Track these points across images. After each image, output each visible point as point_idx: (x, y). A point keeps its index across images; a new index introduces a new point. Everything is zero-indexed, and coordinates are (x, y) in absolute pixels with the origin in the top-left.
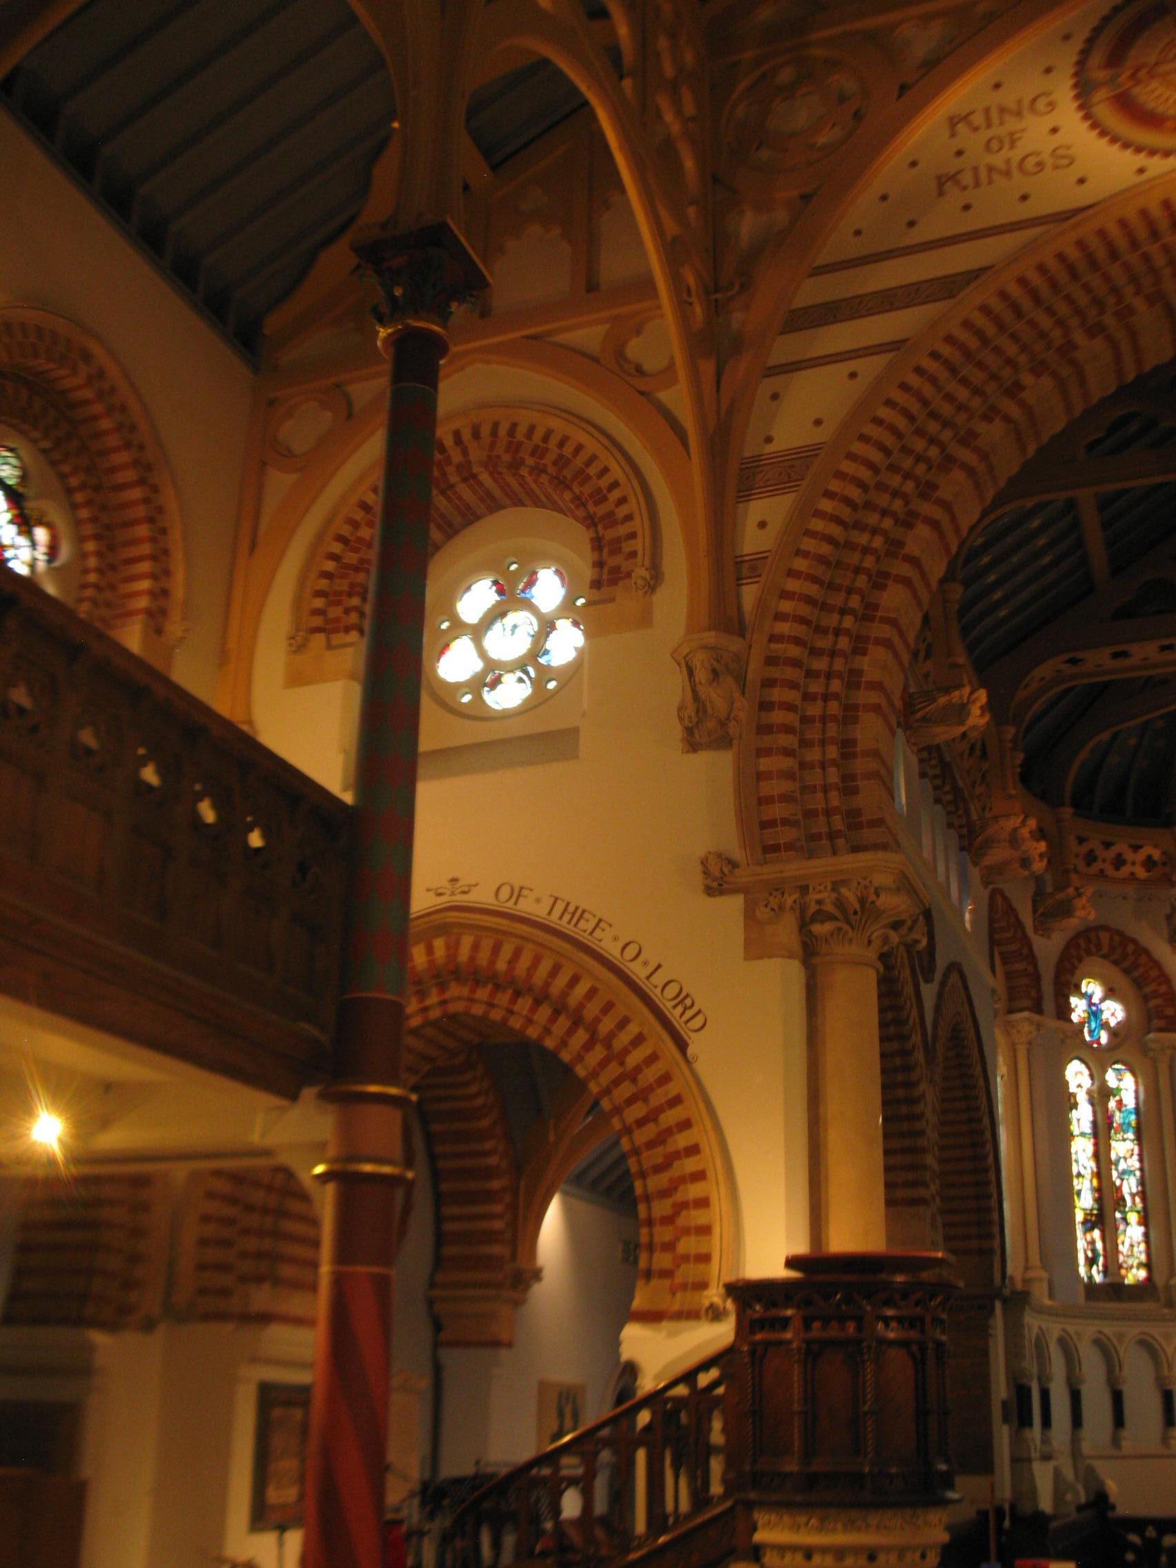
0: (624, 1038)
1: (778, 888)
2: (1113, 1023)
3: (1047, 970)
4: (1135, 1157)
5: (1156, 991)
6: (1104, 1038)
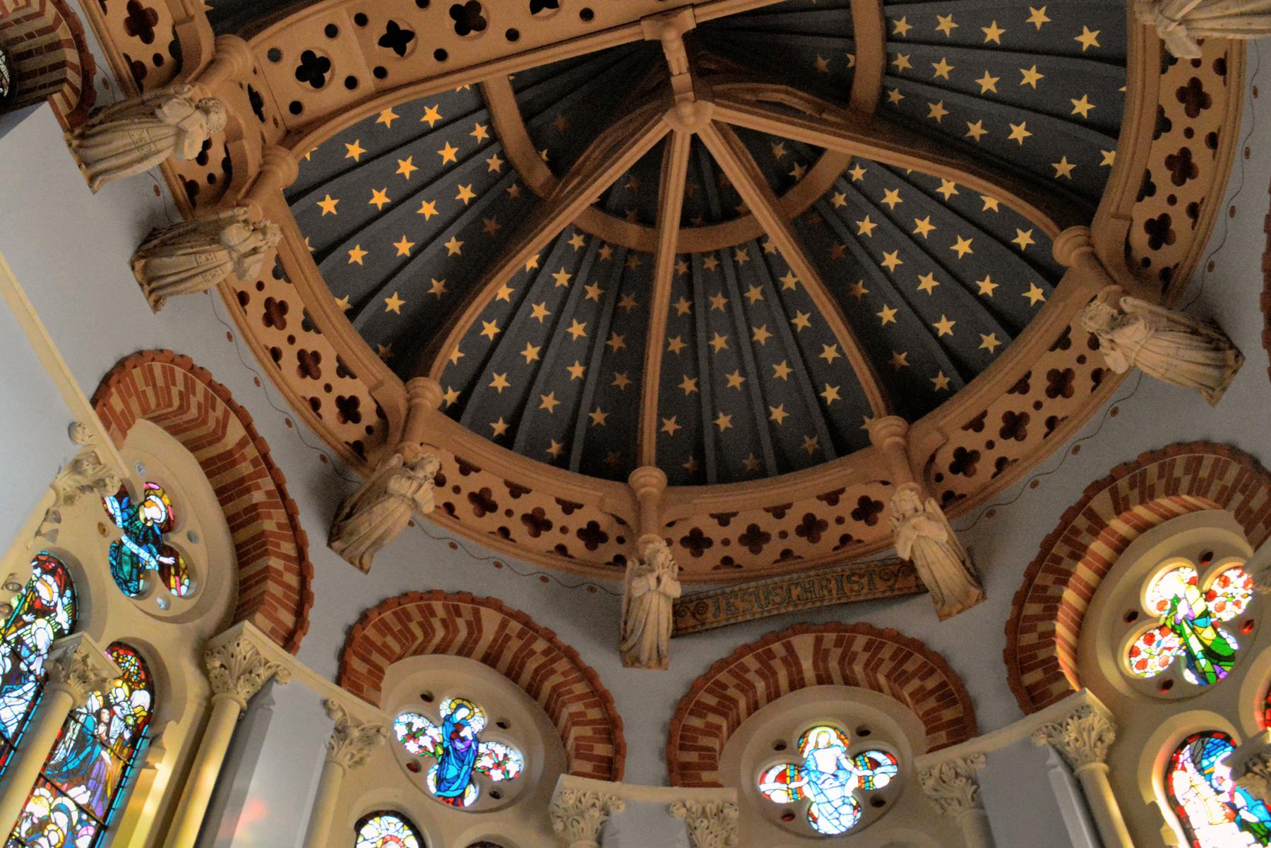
2: (497, 775)
5: (583, 714)
6: (471, 795)
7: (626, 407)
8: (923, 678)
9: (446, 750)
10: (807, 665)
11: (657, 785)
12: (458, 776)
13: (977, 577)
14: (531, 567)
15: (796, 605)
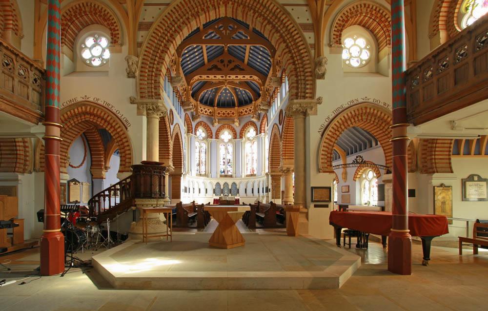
0: (117, 127)
1: (142, 104)
3: (194, 127)
6: (202, 138)
7: (215, 96)
13: (240, 124)
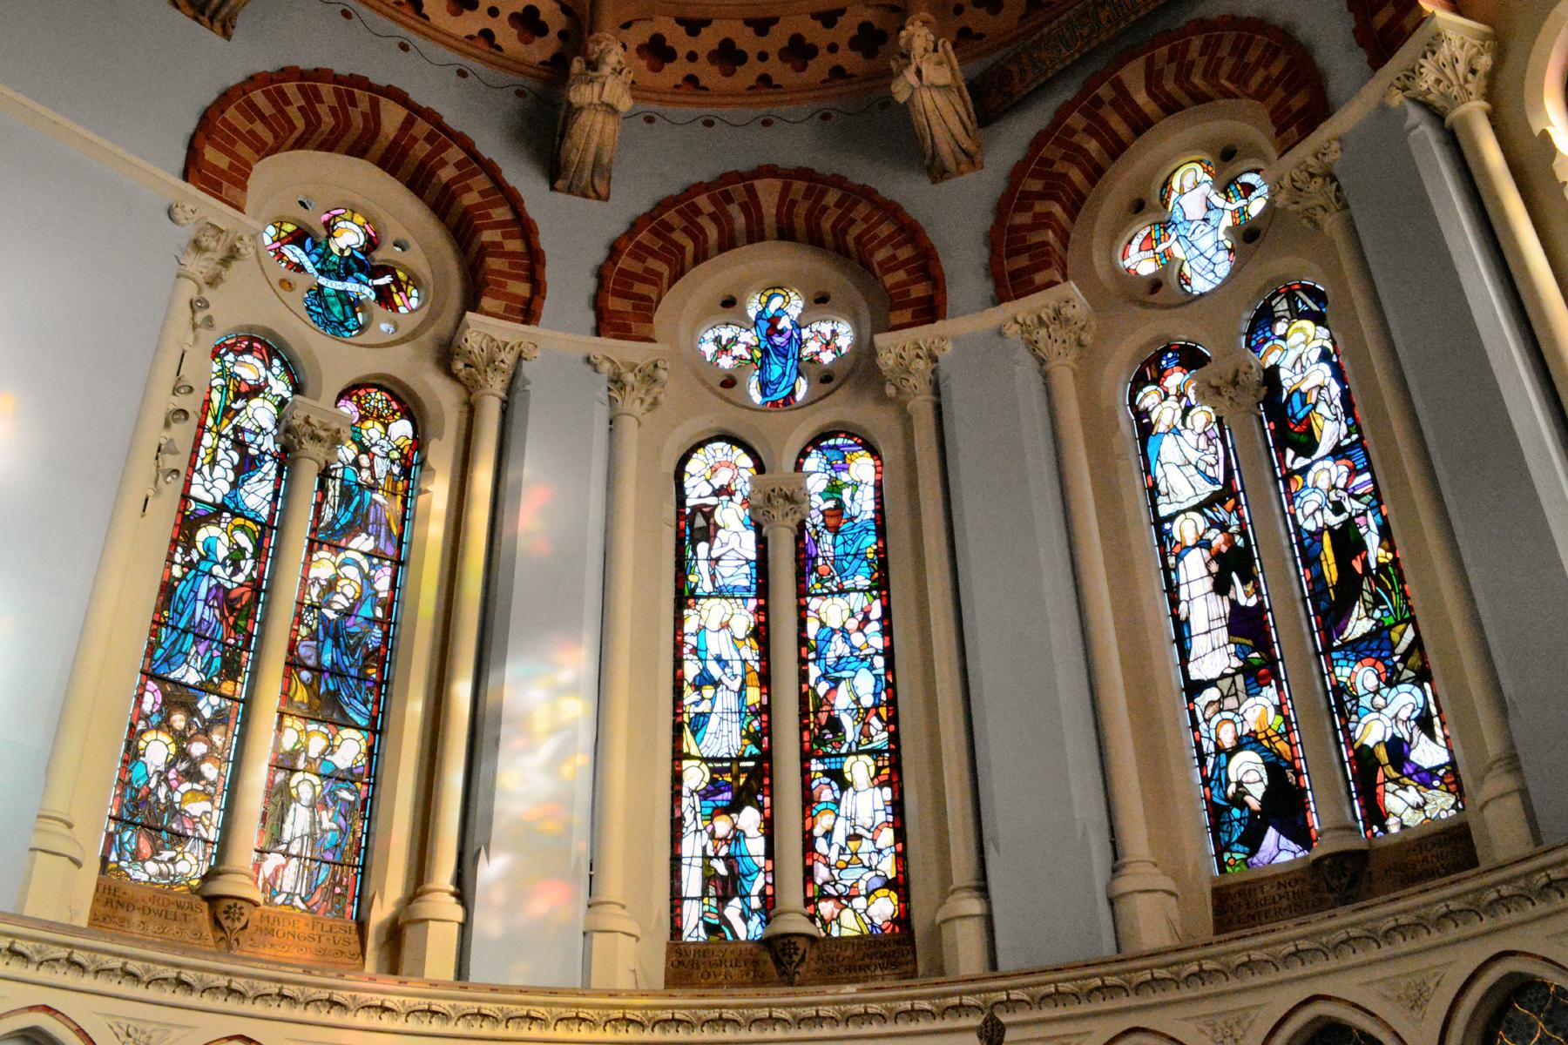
4: (874, 627)
6: (802, 388)
8: (1266, 67)
9: (765, 352)
10: (1142, 98)
11: (983, 310)
12: (784, 374)
14: (806, 109)
15: (1107, 31)
